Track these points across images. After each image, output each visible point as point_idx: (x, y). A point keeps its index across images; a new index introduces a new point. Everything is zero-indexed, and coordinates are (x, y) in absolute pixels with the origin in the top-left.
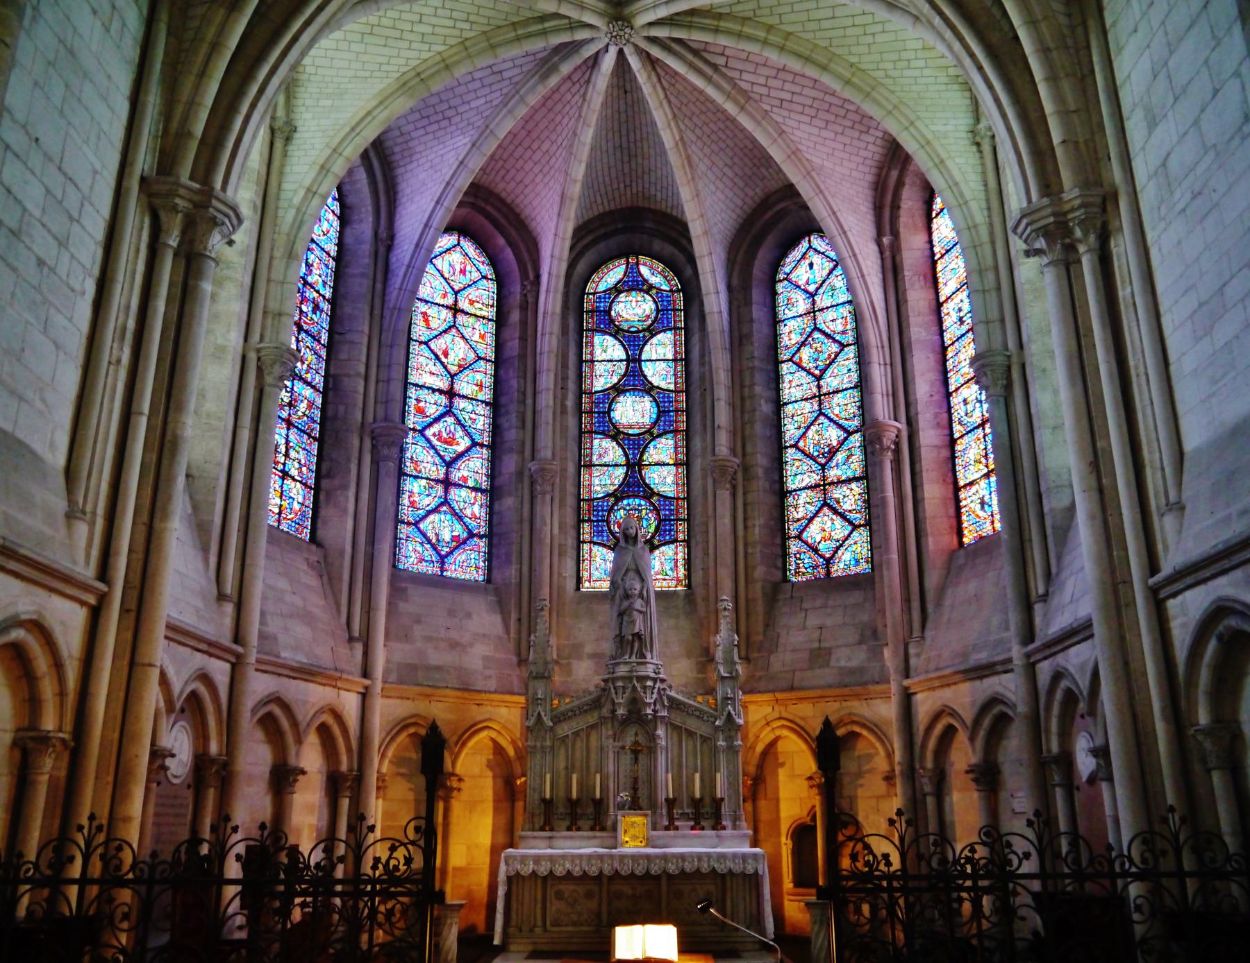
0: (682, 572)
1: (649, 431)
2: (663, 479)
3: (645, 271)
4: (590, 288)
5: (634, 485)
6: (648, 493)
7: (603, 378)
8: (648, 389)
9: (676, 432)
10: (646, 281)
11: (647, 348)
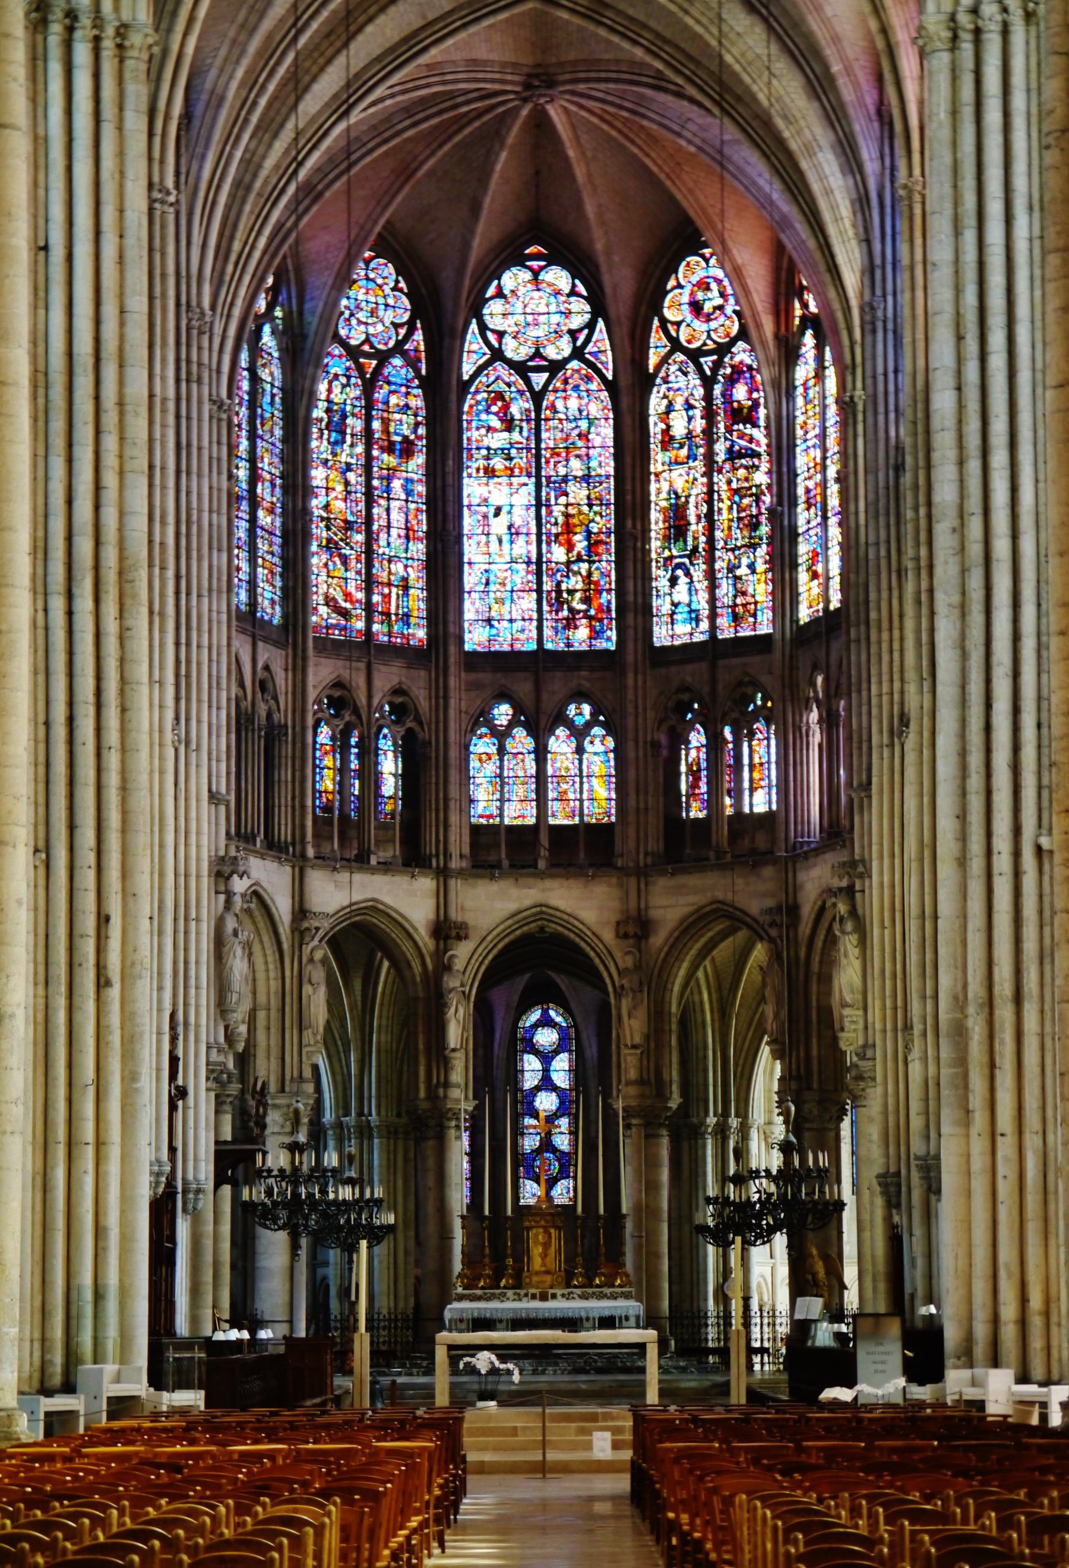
0: (572, 1194)
1: (555, 1114)
2: (562, 1142)
3: (552, 1013)
4: (520, 1025)
5: (547, 1145)
6: (554, 1150)
7: (530, 1081)
8: (554, 1088)
9: (569, 1115)
10: (553, 1020)
11: (554, 1063)
